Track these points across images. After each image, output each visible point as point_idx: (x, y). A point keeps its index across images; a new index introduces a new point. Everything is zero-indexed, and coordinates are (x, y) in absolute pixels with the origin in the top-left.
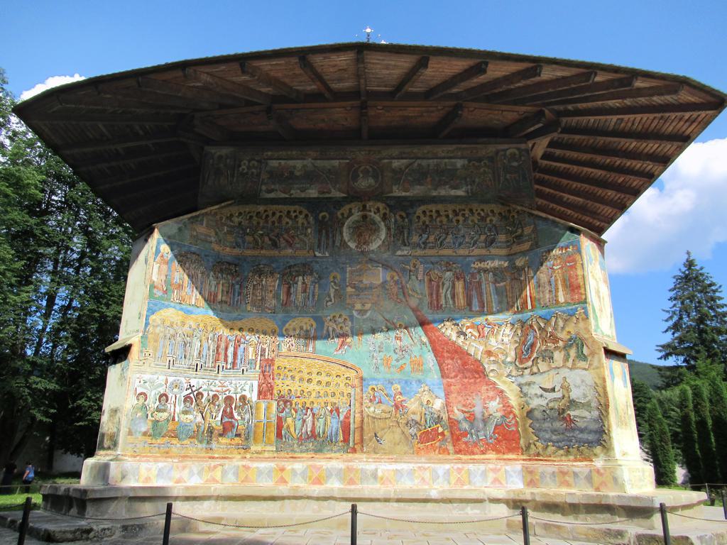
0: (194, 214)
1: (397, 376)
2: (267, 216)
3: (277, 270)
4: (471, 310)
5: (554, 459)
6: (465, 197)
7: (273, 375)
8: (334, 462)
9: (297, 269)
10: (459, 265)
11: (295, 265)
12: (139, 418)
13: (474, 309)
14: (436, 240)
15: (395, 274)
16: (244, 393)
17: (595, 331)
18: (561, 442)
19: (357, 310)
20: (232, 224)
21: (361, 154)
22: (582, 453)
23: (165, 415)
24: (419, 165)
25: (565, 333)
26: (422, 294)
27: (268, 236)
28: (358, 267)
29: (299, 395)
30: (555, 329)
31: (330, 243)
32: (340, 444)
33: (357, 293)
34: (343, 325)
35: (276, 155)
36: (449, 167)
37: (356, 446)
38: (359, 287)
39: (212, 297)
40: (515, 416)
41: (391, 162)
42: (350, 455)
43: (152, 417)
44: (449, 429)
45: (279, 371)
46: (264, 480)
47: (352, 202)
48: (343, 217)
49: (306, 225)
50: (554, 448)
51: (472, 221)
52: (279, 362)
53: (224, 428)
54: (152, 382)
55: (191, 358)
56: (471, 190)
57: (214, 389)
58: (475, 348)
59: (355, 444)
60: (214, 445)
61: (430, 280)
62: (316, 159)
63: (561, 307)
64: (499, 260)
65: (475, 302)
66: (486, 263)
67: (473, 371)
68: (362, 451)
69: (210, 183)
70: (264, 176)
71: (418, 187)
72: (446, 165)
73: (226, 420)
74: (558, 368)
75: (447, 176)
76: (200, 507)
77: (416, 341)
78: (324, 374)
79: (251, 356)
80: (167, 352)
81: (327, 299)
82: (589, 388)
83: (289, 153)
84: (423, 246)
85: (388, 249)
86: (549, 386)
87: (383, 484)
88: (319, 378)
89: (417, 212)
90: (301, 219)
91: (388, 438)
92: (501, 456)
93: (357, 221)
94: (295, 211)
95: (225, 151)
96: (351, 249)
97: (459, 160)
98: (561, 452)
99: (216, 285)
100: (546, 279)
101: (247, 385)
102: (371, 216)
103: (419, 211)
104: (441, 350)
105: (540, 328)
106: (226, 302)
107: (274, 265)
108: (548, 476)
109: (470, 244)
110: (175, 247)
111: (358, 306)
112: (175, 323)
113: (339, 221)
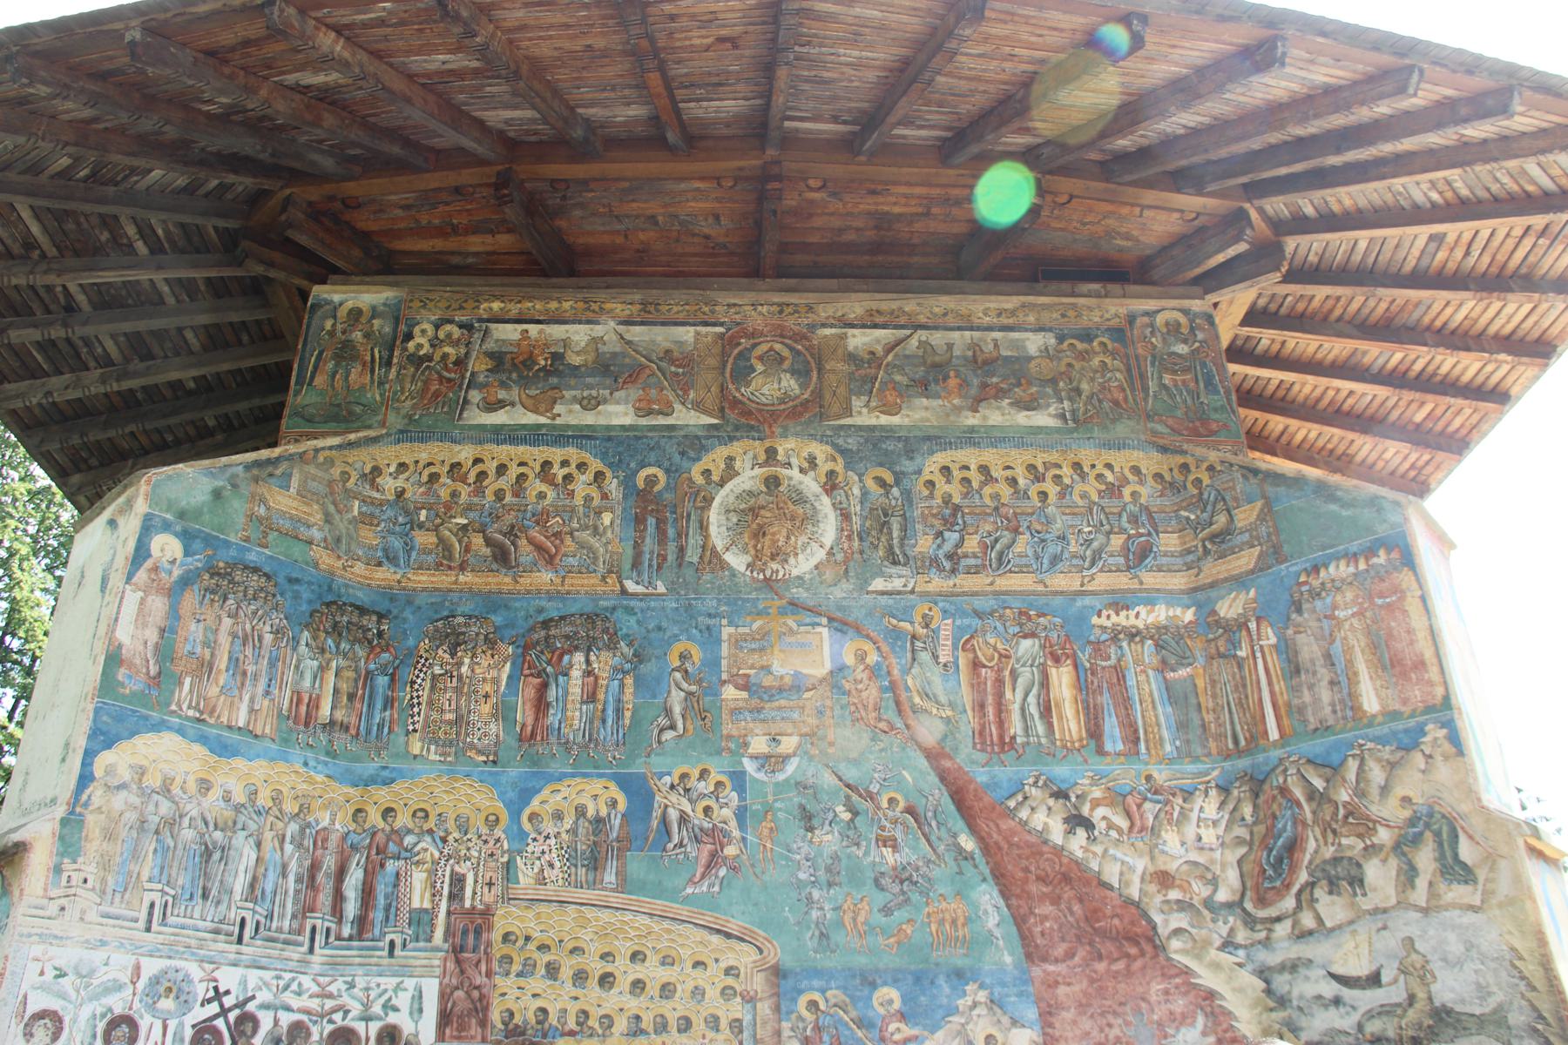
0: (264, 454)
1: (890, 960)
2: (482, 475)
3: (508, 633)
4: (1100, 751)
6: (1057, 430)
7: (489, 960)
9: (568, 629)
11: (562, 618)
13: (1108, 747)
15: (867, 646)
16: (393, 1018)
19: (754, 757)
21: (753, 307)
25: (1393, 800)
26: (951, 705)
28: (756, 626)
29: (572, 1024)
30: (1360, 792)
33: (755, 702)
34: (712, 803)
35: (514, 309)
39: (303, 709)
41: (843, 337)
47: (731, 439)
48: (709, 481)
49: (596, 502)
51: (1084, 496)
55: (225, 898)
56: (1073, 412)
57: (296, 1003)
58: (1121, 865)
61: (976, 665)
62: (628, 322)
63: (1370, 725)
64: (1169, 604)
66: (1132, 613)
69: (320, 380)
70: (478, 365)
72: (996, 346)
74: (1385, 911)
75: (993, 377)
77: (941, 848)
79: (418, 898)
80: (145, 875)
83: (553, 305)
84: (947, 565)
85: (846, 571)
88: (638, 971)
89: (926, 471)
90: (582, 485)
93: (750, 493)
95: (369, 297)
96: (733, 574)
99: (317, 674)
100: (1315, 648)
102: (790, 479)
103: (932, 465)
104: (1020, 874)
105: (1312, 794)
106: (345, 728)
107: (498, 619)
110: (197, 545)
111: (759, 744)
112: (179, 781)
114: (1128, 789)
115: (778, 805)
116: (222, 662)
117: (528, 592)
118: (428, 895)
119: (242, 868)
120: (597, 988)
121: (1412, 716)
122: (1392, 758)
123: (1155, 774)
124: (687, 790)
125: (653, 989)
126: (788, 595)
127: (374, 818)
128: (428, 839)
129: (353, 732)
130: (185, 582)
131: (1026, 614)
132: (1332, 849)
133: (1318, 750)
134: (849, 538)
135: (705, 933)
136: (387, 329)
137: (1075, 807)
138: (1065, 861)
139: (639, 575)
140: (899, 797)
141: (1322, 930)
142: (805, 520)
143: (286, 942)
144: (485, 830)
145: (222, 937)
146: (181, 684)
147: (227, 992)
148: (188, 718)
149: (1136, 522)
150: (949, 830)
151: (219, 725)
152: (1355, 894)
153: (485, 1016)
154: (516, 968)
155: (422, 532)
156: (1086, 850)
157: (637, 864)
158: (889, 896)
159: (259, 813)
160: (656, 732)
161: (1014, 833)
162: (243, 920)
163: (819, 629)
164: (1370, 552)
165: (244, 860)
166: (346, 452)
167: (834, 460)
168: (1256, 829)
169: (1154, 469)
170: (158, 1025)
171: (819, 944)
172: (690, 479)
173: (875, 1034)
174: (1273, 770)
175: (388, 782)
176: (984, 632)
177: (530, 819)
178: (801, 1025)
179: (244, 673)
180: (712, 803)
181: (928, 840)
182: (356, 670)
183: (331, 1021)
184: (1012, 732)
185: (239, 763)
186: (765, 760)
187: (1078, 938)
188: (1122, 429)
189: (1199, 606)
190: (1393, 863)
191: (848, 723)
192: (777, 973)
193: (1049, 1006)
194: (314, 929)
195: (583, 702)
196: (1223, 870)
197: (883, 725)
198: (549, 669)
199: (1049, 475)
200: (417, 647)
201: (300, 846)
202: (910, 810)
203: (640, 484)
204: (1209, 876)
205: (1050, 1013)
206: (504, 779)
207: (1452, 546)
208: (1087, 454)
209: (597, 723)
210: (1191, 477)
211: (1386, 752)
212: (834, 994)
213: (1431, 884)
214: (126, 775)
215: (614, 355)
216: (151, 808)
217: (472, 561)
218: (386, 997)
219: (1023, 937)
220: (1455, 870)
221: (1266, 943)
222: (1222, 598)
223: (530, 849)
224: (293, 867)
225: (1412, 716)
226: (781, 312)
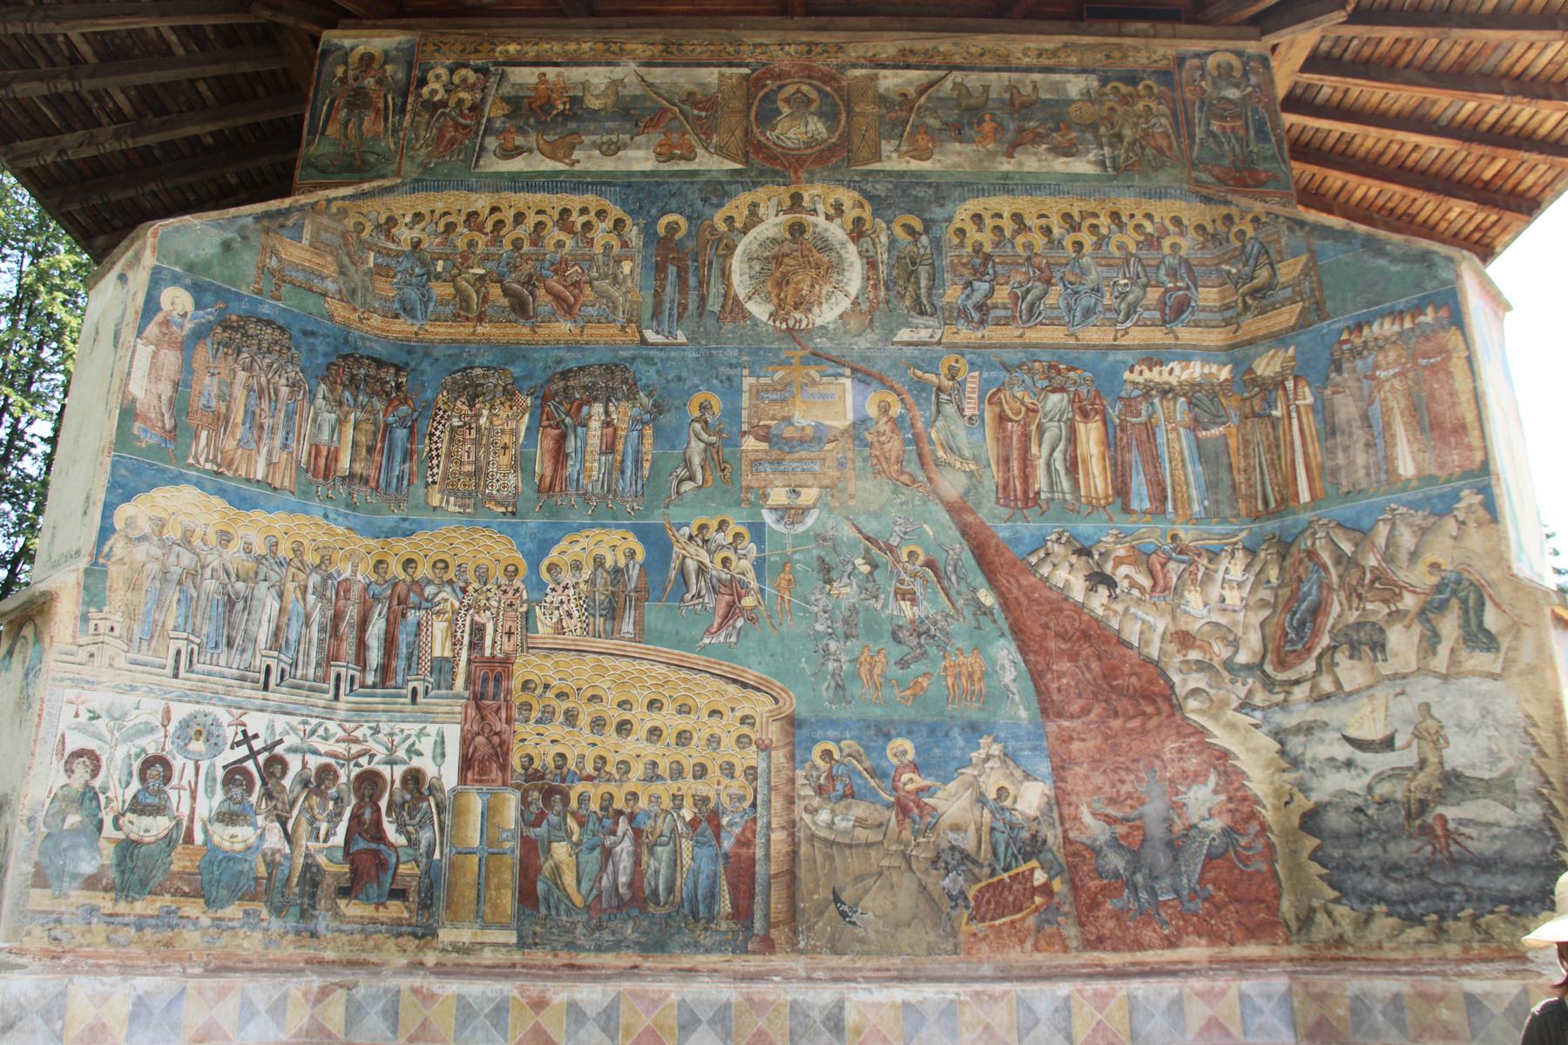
0: (274, 205)
1: (903, 713)
2: (500, 224)
3: (527, 384)
4: (1126, 509)
5: (1394, 955)
6: (1096, 178)
7: (509, 708)
9: (587, 380)
10: (1088, 375)
11: (581, 369)
12: (74, 831)
13: (1135, 505)
15: (892, 398)
16: (416, 762)
18: (1415, 902)
19: (773, 509)
20: (392, 246)
22: (1488, 936)
23: (158, 826)
24: (957, 86)
25: (1421, 568)
26: (976, 459)
28: (777, 377)
29: (589, 769)
32: (724, 926)
33: (775, 454)
34: (730, 554)
35: (531, 51)
36: (1044, 96)
37: (774, 933)
38: (780, 437)
39: (322, 462)
40: (1264, 828)
41: (874, 78)
42: (754, 963)
43: (117, 827)
44: (1066, 875)
45: (526, 697)
47: (755, 184)
48: (732, 229)
49: (616, 250)
50: (1391, 921)
51: (1121, 247)
53: (354, 871)
54: (118, 718)
55: (250, 647)
56: (1114, 159)
58: (1142, 625)
59: (769, 925)
60: (323, 923)
61: (1002, 419)
62: (650, 64)
63: (1404, 489)
64: (1205, 361)
65: (1139, 484)
66: (1166, 369)
67: (1138, 694)
69: (332, 130)
70: (494, 111)
71: (957, 145)
72: (1035, 88)
73: (362, 844)
74: (1404, 676)
75: (1035, 122)
78: (669, 708)
79: (440, 647)
80: (170, 624)
82: (1507, 732)
83: (572, 47)
84: (976, 316)
85: (872, 321)
86: (1375, 732)
88: (655, 719)
89: (957, 218)
91: (873, 905)
92: (1221, 950)
93: (774, 241)
94: (584, 211)
95: (381, 42)
96: (756, 323)
97: (1071, 77)
98: (1417, 932)
99: (336, 428)
100: (1353, 409)
101: (432, 742)
102: (816, 226)
103: (963, 213)
105: (1339, 557)
107: (516, 370)
109: (1118, 312)
111: (779, 496)
112: (199, 532)
113: (720, 240)
114: (1153, 547)
115: (796, 557)
116: (238, 415)
117: (547, 343)
118: (448, 644)
119: (265, 617)
120: (615, 735)
121: (1448, 481)
122: (1424, 524)
123: (1182, 534)
124: (705, 542)
125: (669, 737)
126: (811, 345)
127: (395, 569)
128: (448, 589)
129: (373, 484)
130: (198, 335)
132: (1356, 614)
133: (1348, 514)
134: (875, 286)
136: (400, 75)
138: (1085, 618)
139: (659, 325)
140: (919, 551)
141: (1340, 694)
142: (831, 268)
143: (312, 689)
144: (504, 581)
145: (248, 684)
146: (197, 437)
147: (256, 736)
148: (205, 471)
149: (1174, 275)
150: (969, 585)
151: (237, 478)
152: (1376, 660)
153: (506, 760)
154: (535, 714)
155: (439, 283)
156: (1107, 608)
157: (654, 614)
158: (906, 649)
160: (674, 483)
161: (1034, 589)
162: (268, 669)
163: (842, 380)
164: (1418, 310)
165: (268, 610)
166: (359, 202)
167: (862, 206)
168: (1280, 592)
169: (1197, 220)
171: (835, 695)
172: (712, 227)
173: (888, 783)
174: (1302, 532)
175: (408, 534)
176: (1012, 386)
177: (549, 570)
178: (815, 773)
179: (261, 427)
180: (730, 554)
181: (947, 595)
182: (375, 423)
183: (357, 765)
184: (1037, 487)
185: (258, 515)
186: (784, 512)
187: (1095, 695)
188: (1163, 178)
190: (1417, 629)
191: (870, 475)
193: (1063, 760)
194: (338, 677)
195: (601, 453)
196: (1245, 633)
197: (904, 478)
198: (568, 420)
199: (1085, 224)
200: (435, 399)
201: (322, 596)
202: (930, 564)
203: (661, 231)
204: (1231, 637)
205: (1063, 768)
206: (522, 530)
207: (1507, 307)
208: (1126, 204)
209: (615, 474)
210: (1235, 229)
211: (1419, 518)
212: (849, 744)
213: (1452, 651)
214: (147, 528)
215: (635, 98)
216: (173, 559)
217: (490, 312)
218: (410, 742)
219: (1039, 692)
220: (1478, 637)
221: (1284, 705)
222: (1260, 355)
223: (548, 599)
224: (316, 616)
225: (1448, 481)
226: (809, 52)
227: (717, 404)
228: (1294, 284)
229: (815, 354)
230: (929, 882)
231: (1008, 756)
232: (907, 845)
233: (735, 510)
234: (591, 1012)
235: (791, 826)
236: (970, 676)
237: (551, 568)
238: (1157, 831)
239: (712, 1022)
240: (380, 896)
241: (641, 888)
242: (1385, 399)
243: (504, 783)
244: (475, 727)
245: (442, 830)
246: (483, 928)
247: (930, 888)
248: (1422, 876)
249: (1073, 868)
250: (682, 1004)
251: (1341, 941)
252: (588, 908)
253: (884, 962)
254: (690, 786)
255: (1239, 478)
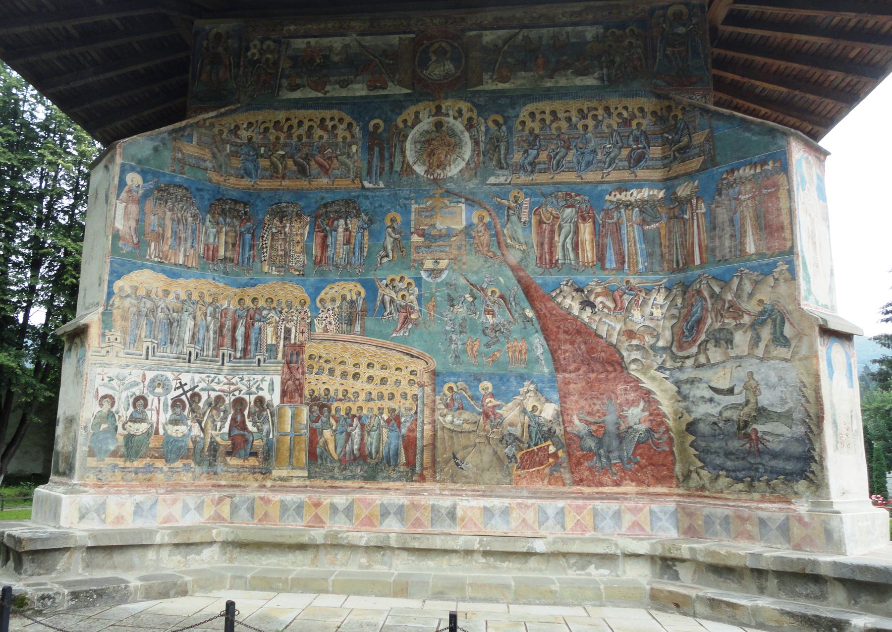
1: (489, 369)
2: (291, 127)
4: (603, 268)
6: (597, 87)
8: (393, 494)
9: (336, 208)
11: (333, 202)
13: (607, 266)
14: (550, 158)
15: (485, 213)
16: (261, 393)
17: (806, 299)
20: (239, 141)
24: (526, 38)
25: (754, 302)
27: (292, 157)
28: (428, 203)
29: (340, 396)
30: (738, 296)
31: (387, 168)
33: (427, 243)
37: (425, 472)
39: (211, 253)
40: (668, 430)
41: (481, 36)
42: (416, 485)
44: (565, 449)
45: (311, 362)
46: (291, 519)
47: (418, 101)
49: (349, 140)
50: (728, 479)
52: (310, 349)
53: (233, 444)
56: (608, 76)
57: (217, 387)
58: (608, 326)
59: (423, 468)
61: (540, 222)
62: (363, 34)
63: (748, 260)
64: (651, 188)
67: (606, 362)
68: (434, 477)
71: (523, 73)
72: (568, 36)
73: (236, 432)
74: (741, 358)
76: (197, 557)
79: (270, 340)
81: (383, 253)
82: (790, 389)
84: (529, 168)
85: (476, 173)
86: (724, 385)
87: (464, 527)
88: (370, 372)
89: (521, 115)
90: (341, 131)
91: (471, 460)
92: (644, 489)
93: (427, 132)
94: (332, 119)
96: (418, 176)
97: (588, 28)
99: (216, 236)
100: (725, 216)
101: (269, 385)
102: (448, 123)
105: (713, 295)
106: (232, 260)
107: (302, 203)
108: (718, 521)
111: (429, 264)
113: (400, 133)
114: (616, 288)
117: (317, 189)
119: (187, 329)
121: (771, 257)
123: (632, 281)
124: (394, 287)
125: (377, 380)
127: (248, 303)
131: (570, 194)
133: (718, 272)
134: (478, 155)
135: (401, 355)
137: (586, 296)
138: (579, 323)
140: (497, 290)
141: (708, 365)
142: (455, 146)
143: (211, 361)
144: (299, 307)
152: (728, 348)
154: (315, 370)
155: (263, 159)
156: (590, 318)
157: (370, 322)
159: (193, 303)
161: (554, 309)
162: (190, 353)
163: (460, 205)
166: (220, 119)
167: (472, 111)
169: (652, 109)
170: (156, 399)
172: (396, 125)
174: (695, 281)
177: (320, 302)
189: (668, 189)
191: (473, 253)
192: (435, 374)
194: (223, 355)
197: (490, 254)
199: (590, 115)
201: (214, 317)
202: (502, 297)
203: (371, 128)
204: (655, 333)
206: (307, 283)
208: (613, 102)
210: (672, 114)
211: (755, 276)
213: (766, 346)
217: (288, 174)
219: (554, 360)
220: (780, 340)
221: (681, 369)
222: (680, 185)
224: (212, 326)
226: (446, 22)
227: (399, 219)
228: (701, 146)
229: (447, 191)
230: (499, 450)
231: (538, 391)
232: (488, 432)
233: (407, 272)
234: (341, 508)
235: (433, 423)
236: (520, 352)
237: (322, 300)
238: (612, 428)
239: (396, 513)
240: (245, 455)
241: (364, 451)
242: (742, 211)
243: (301, 403)
244: (288, 377)
245: (273, 424)
246: (292, 469)
247: (499, 452)
248: (743, 459)
249: (569, 445)
250: (382, 505)
251: (703, 488)
252: (340, 460)
253: (476, 488)
254: (387, 404)
255: (665, 250)
